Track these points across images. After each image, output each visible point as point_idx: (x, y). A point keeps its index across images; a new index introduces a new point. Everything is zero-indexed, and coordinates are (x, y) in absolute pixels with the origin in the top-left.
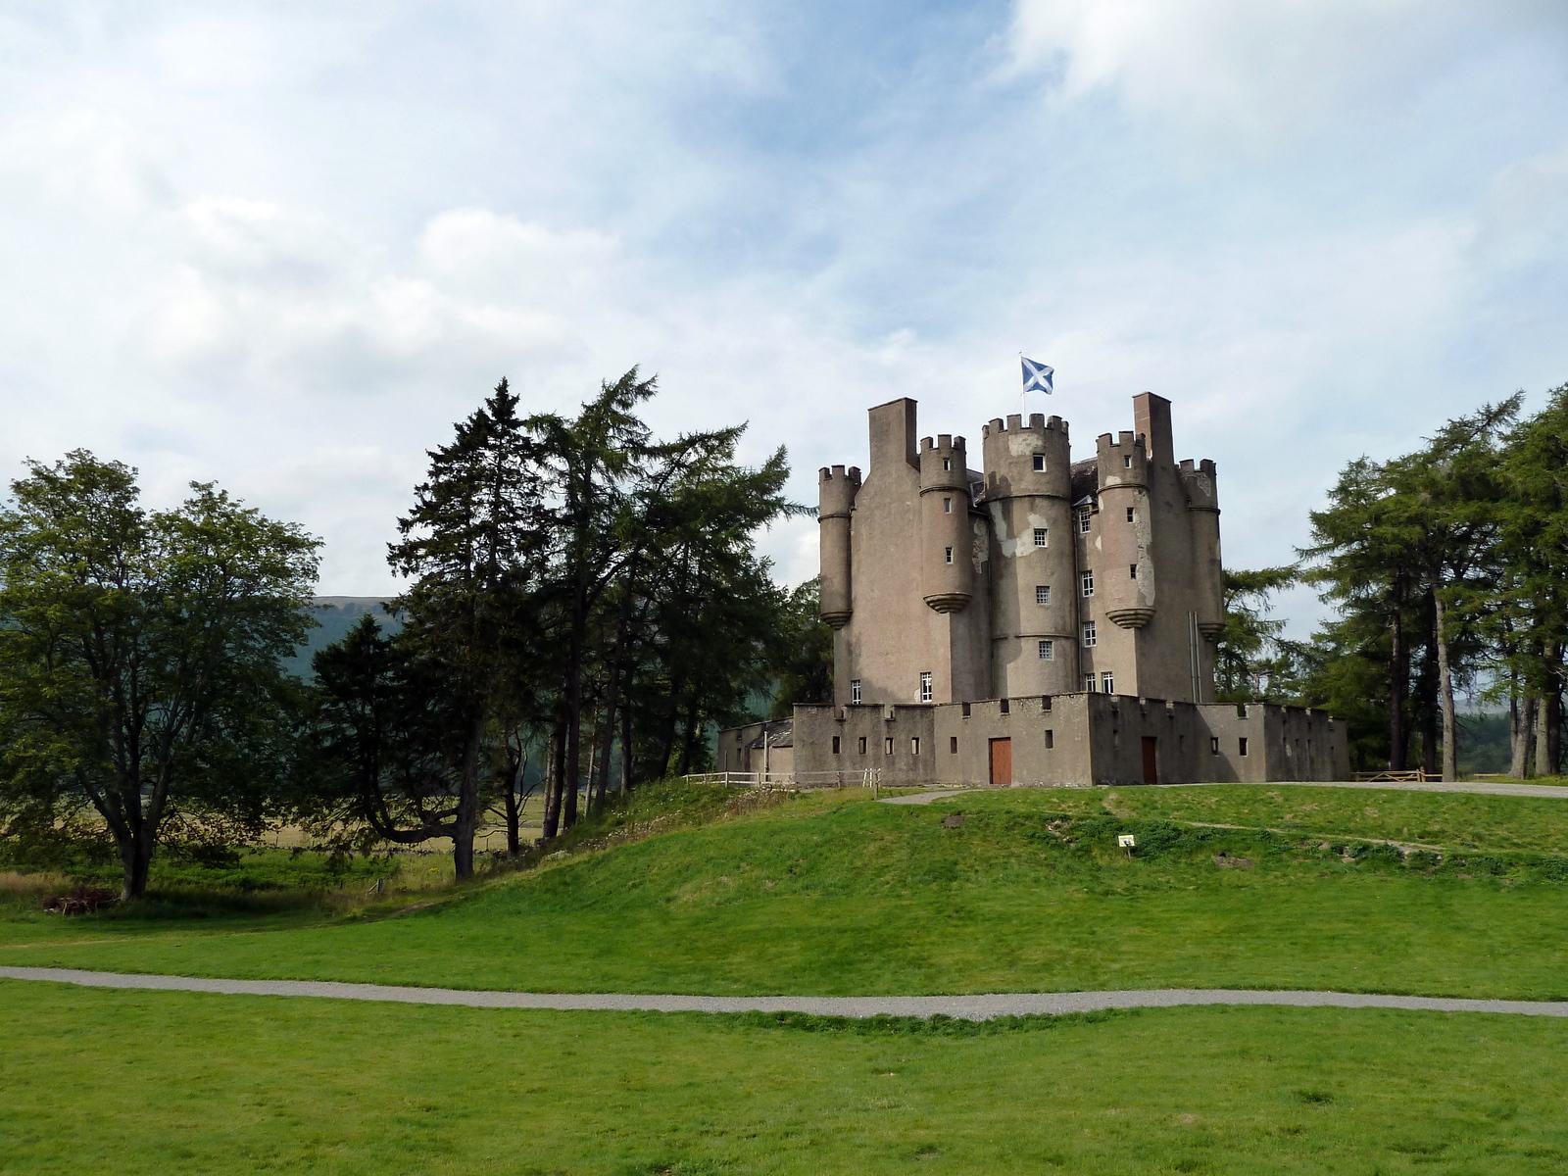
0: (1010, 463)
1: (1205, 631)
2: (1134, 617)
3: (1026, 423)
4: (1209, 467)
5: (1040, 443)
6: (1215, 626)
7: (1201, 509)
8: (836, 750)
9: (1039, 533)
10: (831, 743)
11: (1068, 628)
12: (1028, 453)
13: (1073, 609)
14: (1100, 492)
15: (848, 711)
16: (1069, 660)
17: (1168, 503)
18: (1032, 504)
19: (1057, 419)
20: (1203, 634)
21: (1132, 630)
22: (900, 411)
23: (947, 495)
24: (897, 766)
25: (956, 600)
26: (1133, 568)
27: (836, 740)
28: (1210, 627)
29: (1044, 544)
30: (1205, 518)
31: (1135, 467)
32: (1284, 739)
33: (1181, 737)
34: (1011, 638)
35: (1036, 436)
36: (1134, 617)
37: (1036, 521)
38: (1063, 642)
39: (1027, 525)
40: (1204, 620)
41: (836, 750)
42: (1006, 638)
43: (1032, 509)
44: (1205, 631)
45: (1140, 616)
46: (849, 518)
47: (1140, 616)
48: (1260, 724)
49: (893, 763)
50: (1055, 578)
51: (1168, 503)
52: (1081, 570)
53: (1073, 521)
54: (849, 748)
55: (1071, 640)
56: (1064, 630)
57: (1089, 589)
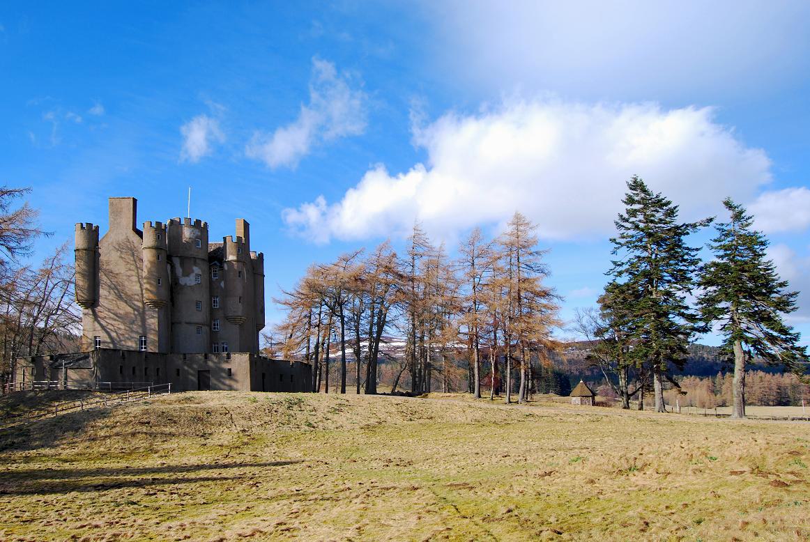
5: (199, 234)
21: (238, 326)
27: (121, 367)
39: (193, 271)
41: (121, 372)
43: (195, 264)
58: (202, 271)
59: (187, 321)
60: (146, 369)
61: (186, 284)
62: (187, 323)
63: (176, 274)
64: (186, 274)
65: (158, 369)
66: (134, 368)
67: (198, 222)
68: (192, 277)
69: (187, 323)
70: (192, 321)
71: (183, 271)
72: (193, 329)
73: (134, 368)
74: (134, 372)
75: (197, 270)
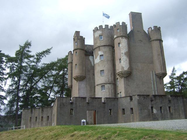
1: (158, 76)
2: (121, 74)
4: (157, 30)
7: (153, 40)
8: (31, 121)
10: (29, 118)
11: (110, 81)
12: (98, 36)
13: (112, 75)
16: (111, 90)
18: (99, 49)
20: (157, 76)
21: (123, 79)
24: (43, 124)
25: (78, 78)
27: (31, 118)
28: (159, 74)
30: (155, 44)
32: (152, 108)
36: (121, 74)
37: (100, 53)
38: (108, 85)
41: (31, 121)
43: (99, 50)
44: (158, 76)
45: (123, 74)
46: (72, 63)
49: (42, 124)
51: (140, 40)
53: (113, 51)
54: (33, 120)
55: (111, 84)
60: (42, 117)
65: (48, 117)
75: (100, 53)
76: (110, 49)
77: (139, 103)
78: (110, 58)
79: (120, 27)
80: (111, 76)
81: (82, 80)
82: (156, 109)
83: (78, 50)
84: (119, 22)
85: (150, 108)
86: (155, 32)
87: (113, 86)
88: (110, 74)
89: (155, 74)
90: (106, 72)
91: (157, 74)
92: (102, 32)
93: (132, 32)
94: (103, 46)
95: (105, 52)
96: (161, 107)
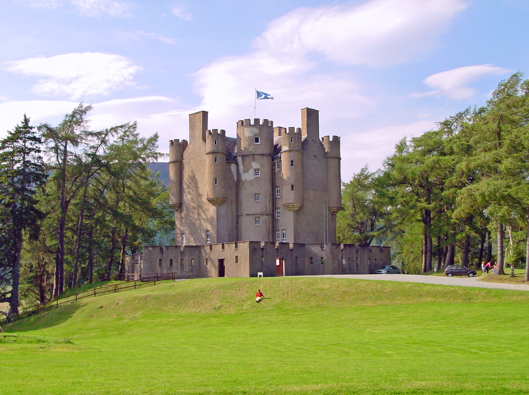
0: (245, 140)
1: (331, 210)
2: (292, 206)
3: (252, 123)
4: (336, 141)
5: (258, 131)
6: (335, 208)
8: (160, 264)
9: (256, 171)
10: (158, 261)
11: (268, 210)
13: (271, 202)
14: (282, 152)
15: (165, 249)
16: (268, 224)
17: (315, 156)
18: (253, 158)
19: (266, 121)
21: (292, 212)
22: (200, 117)
23: (216, 155)
24: (185, 270)
26: (292, 186)
27: (160, 260)
29: (258, 175)
30: (332, 163)
31: (295, 142)
32: (342, 258)
33: (297, 257)
34: (244, 215)
35: (256, 128)
36: (292, 206)
39: (251, 167)
40: (329, 206)
41: (160, 264)
42: (242, 215)
43: (254, 160)
44: (331, 210)
45: (295, 206)
46: (181, 162)
47: (295, 206)
48: (328, 251)
50: (264, 188)
52: (276, 186)
53: (272, 165)
56: (266, 211)
57: (279, 194)
58: (260, 165)
59: (247, 212)
61: (246, 180)
62: (246, 215)
63: (239, 171)
64: (246, 171)
66: (171, 260)
67: (257, 121)
68: (251, 172)
69: (246, 215)
70: (251, 213)
71: (244, 167)
72: (251, 219)
73: (171, 260)
74: (171, 264)
75: (255, 165)
76: (269, 161)
77: (332, 252)
78: (268, 175)
79: (295, 135)
80: (269, 204)
81: (222, 204)
82: (345, 260)
83: (219, 155)
84: (294, 128)
85: (340, 258)
86: (334, 144)
87: (271, 219)
88: (268, 200)
89: (328, 208)
90: (262, 198)
91: (331, 208)
92: (260, 131)
93: (306, 140)
94: (261, 154)
95: (262, 165)
96: (349, 258)
